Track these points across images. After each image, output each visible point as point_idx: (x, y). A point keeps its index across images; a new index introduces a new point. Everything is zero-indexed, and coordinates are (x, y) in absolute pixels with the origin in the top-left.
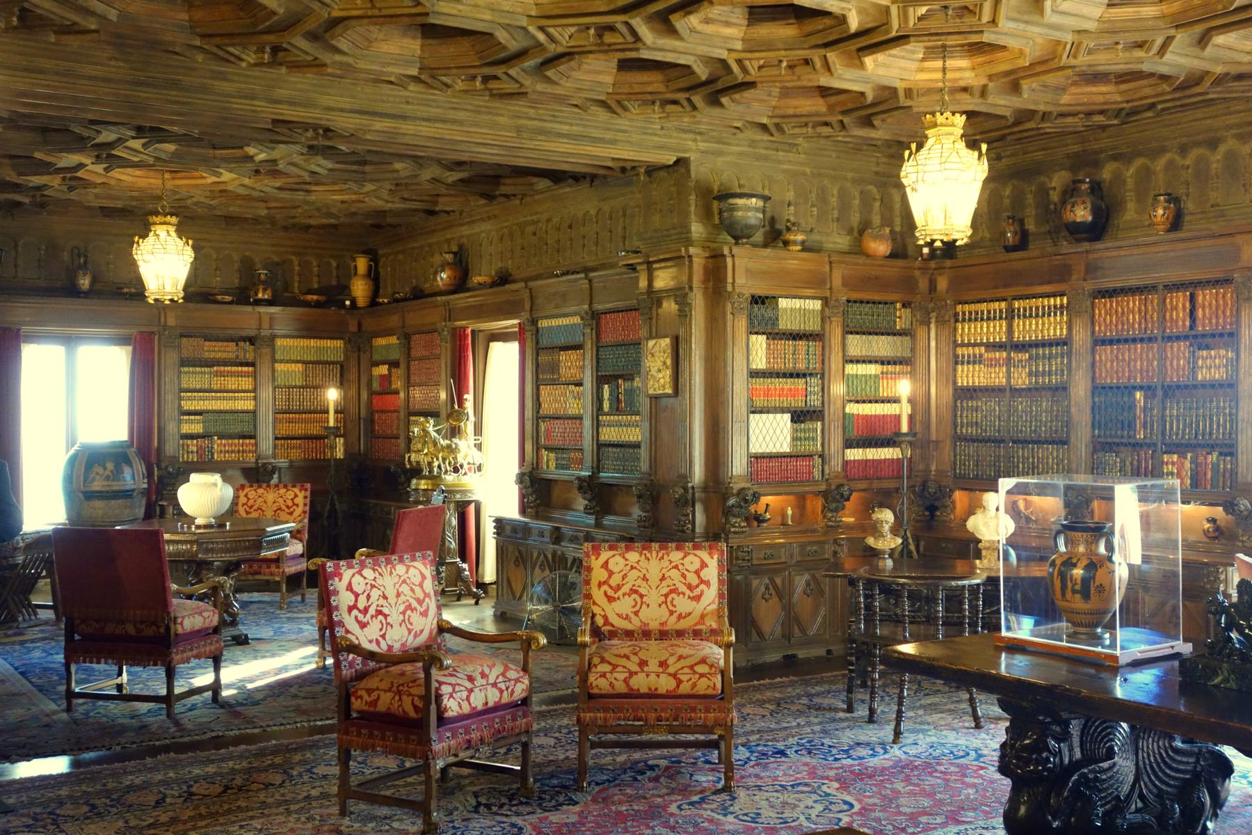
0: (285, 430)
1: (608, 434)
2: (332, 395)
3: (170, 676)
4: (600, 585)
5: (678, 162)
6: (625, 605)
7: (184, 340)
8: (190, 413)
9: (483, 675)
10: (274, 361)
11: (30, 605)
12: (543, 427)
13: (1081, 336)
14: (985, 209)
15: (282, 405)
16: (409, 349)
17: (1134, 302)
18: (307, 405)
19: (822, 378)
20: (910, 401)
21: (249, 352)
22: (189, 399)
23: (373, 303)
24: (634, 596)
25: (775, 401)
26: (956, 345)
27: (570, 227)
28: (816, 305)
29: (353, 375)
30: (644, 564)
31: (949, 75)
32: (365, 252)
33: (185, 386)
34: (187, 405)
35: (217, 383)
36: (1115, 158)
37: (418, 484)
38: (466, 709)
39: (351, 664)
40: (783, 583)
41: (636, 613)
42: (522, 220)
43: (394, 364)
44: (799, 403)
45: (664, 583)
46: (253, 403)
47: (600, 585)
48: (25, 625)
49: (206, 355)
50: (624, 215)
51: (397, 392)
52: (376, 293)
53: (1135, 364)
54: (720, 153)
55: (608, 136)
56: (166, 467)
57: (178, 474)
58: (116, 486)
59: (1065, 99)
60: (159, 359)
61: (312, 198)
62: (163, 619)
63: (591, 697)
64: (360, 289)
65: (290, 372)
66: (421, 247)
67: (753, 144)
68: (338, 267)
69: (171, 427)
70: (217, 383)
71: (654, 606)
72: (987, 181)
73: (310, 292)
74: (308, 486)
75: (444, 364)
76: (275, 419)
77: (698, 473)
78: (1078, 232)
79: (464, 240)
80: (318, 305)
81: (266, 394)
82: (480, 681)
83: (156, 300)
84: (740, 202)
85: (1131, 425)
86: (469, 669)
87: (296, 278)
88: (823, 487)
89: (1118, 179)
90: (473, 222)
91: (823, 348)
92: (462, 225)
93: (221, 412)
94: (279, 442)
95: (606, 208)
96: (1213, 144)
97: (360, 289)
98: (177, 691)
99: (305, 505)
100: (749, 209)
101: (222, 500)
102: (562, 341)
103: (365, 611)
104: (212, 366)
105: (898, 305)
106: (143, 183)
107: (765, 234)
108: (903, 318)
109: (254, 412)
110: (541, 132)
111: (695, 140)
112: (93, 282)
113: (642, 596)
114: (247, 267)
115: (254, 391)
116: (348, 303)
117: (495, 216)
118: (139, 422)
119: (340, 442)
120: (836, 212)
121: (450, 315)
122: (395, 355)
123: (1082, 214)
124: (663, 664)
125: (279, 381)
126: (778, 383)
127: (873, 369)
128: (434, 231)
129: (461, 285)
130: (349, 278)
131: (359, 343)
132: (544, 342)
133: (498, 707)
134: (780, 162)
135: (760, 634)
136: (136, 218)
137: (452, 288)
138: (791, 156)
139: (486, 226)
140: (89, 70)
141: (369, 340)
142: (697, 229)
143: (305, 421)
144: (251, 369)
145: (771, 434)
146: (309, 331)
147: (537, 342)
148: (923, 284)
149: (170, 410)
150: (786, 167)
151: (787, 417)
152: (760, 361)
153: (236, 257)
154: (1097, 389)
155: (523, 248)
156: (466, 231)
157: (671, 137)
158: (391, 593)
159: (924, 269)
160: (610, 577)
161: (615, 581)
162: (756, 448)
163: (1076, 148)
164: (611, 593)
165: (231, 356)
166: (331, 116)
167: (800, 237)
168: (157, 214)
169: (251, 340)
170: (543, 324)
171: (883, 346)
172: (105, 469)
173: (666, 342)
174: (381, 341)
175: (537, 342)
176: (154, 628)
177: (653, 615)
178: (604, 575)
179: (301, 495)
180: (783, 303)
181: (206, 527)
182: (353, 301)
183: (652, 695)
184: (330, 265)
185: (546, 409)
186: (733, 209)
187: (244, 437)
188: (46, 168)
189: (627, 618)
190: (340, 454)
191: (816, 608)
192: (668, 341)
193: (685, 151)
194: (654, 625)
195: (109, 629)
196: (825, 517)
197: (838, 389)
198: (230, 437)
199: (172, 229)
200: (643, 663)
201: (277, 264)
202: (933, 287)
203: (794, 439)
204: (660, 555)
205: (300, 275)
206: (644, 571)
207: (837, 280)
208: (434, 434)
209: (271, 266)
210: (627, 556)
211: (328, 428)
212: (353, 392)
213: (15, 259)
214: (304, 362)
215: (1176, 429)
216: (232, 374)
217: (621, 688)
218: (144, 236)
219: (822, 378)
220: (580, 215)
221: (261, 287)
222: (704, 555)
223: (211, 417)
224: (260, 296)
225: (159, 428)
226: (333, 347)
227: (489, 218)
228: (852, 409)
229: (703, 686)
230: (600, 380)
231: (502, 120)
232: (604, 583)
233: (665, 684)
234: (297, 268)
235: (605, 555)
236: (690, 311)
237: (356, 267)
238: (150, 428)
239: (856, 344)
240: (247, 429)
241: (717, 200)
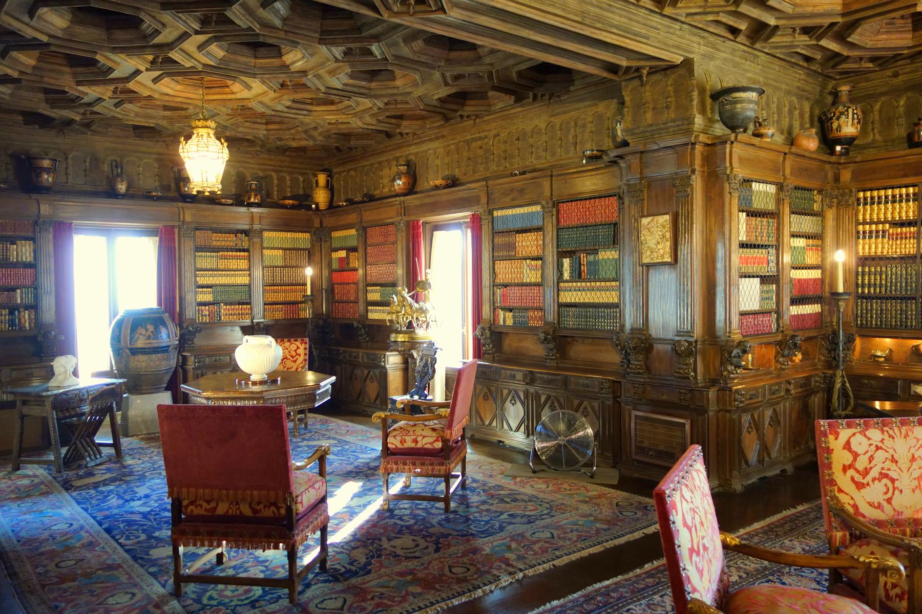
0: (272, 297)
1: (568, 297)
4: (845, 469)
6: (876, 492)
7: (198, 232)
8: (203, 287)
10: (263, 248)
11: (93, 442)
12: (499, 292)
16: (366, 238)
18: (286, 280)
19: (777, 250)
21: (244, 242)
22: (202, 276)
23: (331, 206)
24: (885, 481)
27: (518, 139)
30: (888, 442)
32: (323, 170)
33: (198, 266)
34: (201, 281)
35: (222, 264)
37: (396, 337)
40: (759, 417)
41: (889, 501)
42: (469, 137)
45: (915, 465)
46: (248, 278)
47: (845, 469)
48: (93, 464)
49: (214, 243)
50: (576, 125)
51: (356, 270)
56: (187, 327)
57: (196, 332)
58: (155, 343)
60: (179, 247)
62: (285, 499)
64: (321, 197)
65: (274, 256)
66: (372, 165)
68: (304, 182)
69: (189, 297)
70: (222, 264)
71: (907, 491)
73: (285, 198)
74: (307, 340)
76: (264, 290)
79: (412, 157)
81: (258, 273)
83: (198, 192)
87: (275, 189)
88: (779, 338)
90: (424, 142)
91: (779, 224)
92: (410, 145)
93: (221, 285)
94: (267, 307)
95: (557, 121)
97: (321, 197)
99: (305, 354)
101: (275, 358)
102: (519, 226)
104: (218, 252)
105: (815, 192)
111: (699, 44)
112: (128, 188)
113: (893, 481)
115: (249, 269)
116: (314, 206)
117: (443, 136)
118: (165, 294)
120: (776, 116)
121: (406, 210)
122: (353, 243)
128: (384, 152)
130: (312, 189)
131: (321, 235)
132: (499, 227)
134: (746, 70)
135: (747, 462)
137: (405, 191)
143: (285, 291)
144: (246, 254)
146: (286, 226)
147: (493, 228)
150: (750, 75)
151: (757, 280)
155: (469, 159)
156: (413, 149)
157: (683, 38)
160: (855, 460)
161: (862, 463)
164: (858, 478)
165: (232, 244)
169: (246, 233)
172: (147, 330)
175: (493, 228)
176: (273, 508)
178: (847, 458)
179: (302, 347)
180: (755, 186)
181: (262, 383)
182: (317, 205)
184: (298, 179)
187: (243, 304)
188: (102, 75)
189: (879, 506)
191: (775, 435)
192: (667, 217)
193: (691, 52)
196: (777, 361)
197: (787, 259)
198: (231, 304)
199: (212, 132)
201: (262, 178)
202: (837, 179)
203: (762, 299)
204: (904, 432)
205: (278, 186)
206: (891, 452)
208: (410, 300)
210: (868, 433)
213: (66, 168)
214: (284, 249)
216: (233, 258)
218: (188, 137)
219: (777, 250)
220: (529, 129)
221: (253, 194)
223: (219, 289)
224: (252, 200)
225: (181, 298)
227: (437, 138)
230: (562, 255)
232: (851, 466)
234: (276, 182)
235: (845, 434)
236: (692, 191)
237: (317, 181)
238: (174, 298)
240: (244, 298)
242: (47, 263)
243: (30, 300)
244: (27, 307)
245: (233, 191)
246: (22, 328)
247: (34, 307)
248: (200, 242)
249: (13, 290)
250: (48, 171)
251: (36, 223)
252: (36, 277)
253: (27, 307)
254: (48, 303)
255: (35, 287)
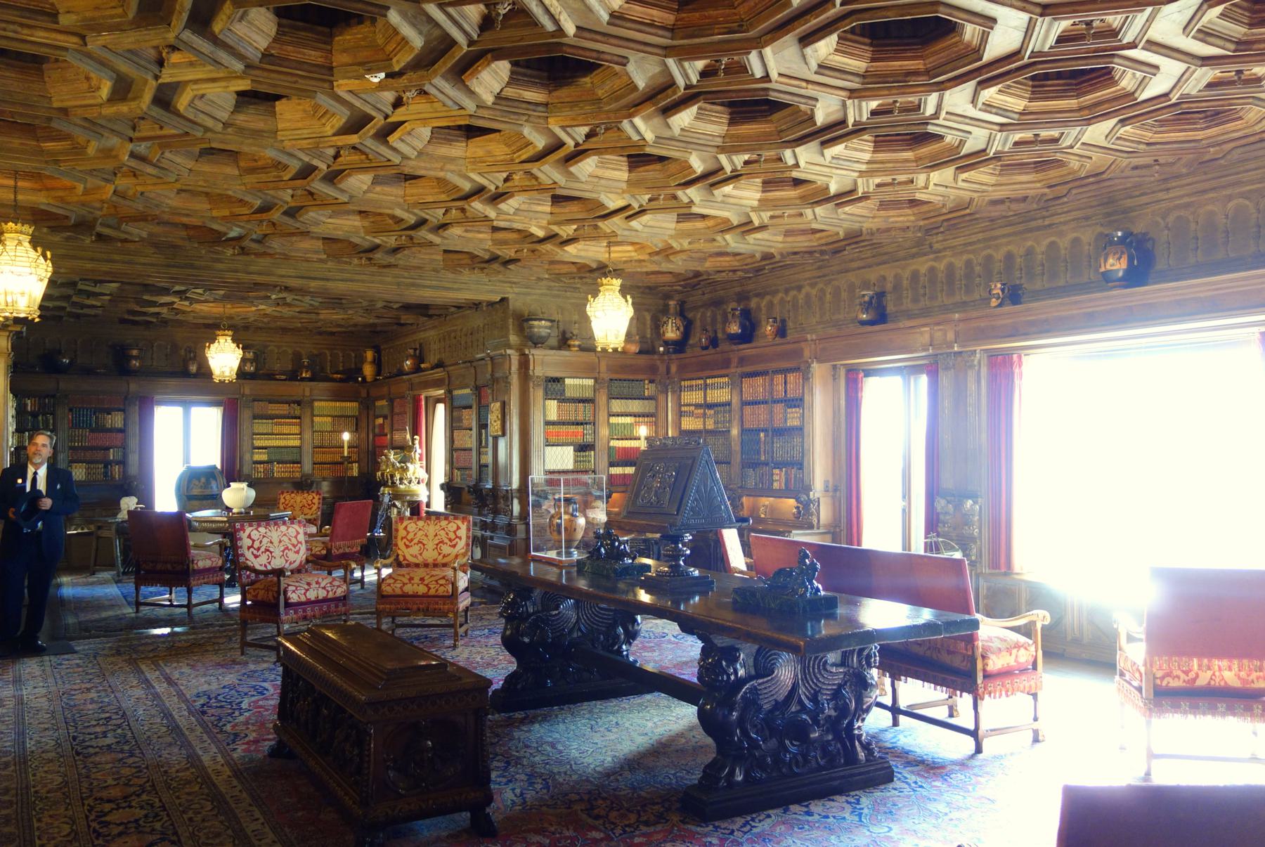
0: (319, 458)
2: (346, 436)
3: (190, 592)
5: (503, 300)
9: (317, 583)
13: (735, 401)
14: (634, 331)
15: (317, 443)
17: (760, 380)
20: (646, 438)
21: (297, 410)
25: (563, 439)
26: (681, 406)
28: (591, 382)
29: (364, 424)
31: (612, 255)
34: (257, 443)
35: (277, 429)
36: (757, 295)
38: (303, 599)
39: (248, 577)
43: (385, 417)
44: (579, 439)
52: (378, 373)
53: (756, 417)
54: (529, 294)
55: (456, 286)
58: (208, 492)
59: (707, 264)
61: (322, 317)
63: (383, 596)
64: (368, 370)
65: (323, 422)
67: (549, 288)
69: (247, 457)
70: (277, 429)
72: (632, 319)
73: (337, 373)
75: (408, 418)
77: (515, 484)
78: (733, 338)
80: (341, 380)
82: (314, 585)
84: (536, 323)
85: (759, 453)
86: (309, 580)
89: (759, 308)
96: (799, 288)
97: (368, 370)
98: (194, 602)
100: (540, 327)
101: (247, 498)
103: (258, 549)
106: (215, 310)
107: (559, 341)
108: (649, 389)
109: (300, 447)
110: (413, 285)
114: (297, 357)
119: (355, 466)
122: (386, 411)
123: (734, 328)
124: (422, 579)
125: (316, 428)
126: (564, 428)
127: (629, 420)
129: (417, 369)
131: (367, 405)
132: (456, 404)
133: (325, 600)
136: (210, 330)
138: (576, 295)
139: (432, 333)
140: (142, 260)
141: (374, 402)
142: (513, 339)
145: (562, 458)
146: (337, 397)
148: (662, 369)
149: (246, 446)
151: (572, 448)
152: (553, 415)
153: (290, 351)
154: (744, 431)
156: (422, 335)
158: (276, 541)
159: (663, 361)
161: (409, 537)
162: (550, 467)
163: (738, 289)
166: (284, 280)
167: (577, 343)
168: (220, 329)
170: (456, 393)
171: (635, 406)
173: (498, 404)
174: (379, 403)
177: (430, 555)
183: (415, 596)
185: (457, 444)
186: (531, 327)
190: (355, 473)
194: (430, 561)
195: (159, 567)
197: (604, 432)
199: (229, 339)
200: (411, 579)
207: (603, 368)
209: (312, 357)
211: (343, 457)
212: (364, 435)
215: (779, 455)
216: (287, 424)
217: (398, 592)
222: (459, 522)
226: (352, 407)
228: (614, 443)
229: (441, 591)
231: (389, 279)
233: (422, 589)
238: (234, 457)
239: (617, 405)
240: (295, 457)
241: (523, 321)
242: (134, 429)
243: (119, 457)
244: (118, 463)
245: (290, 367)
246: (113, 478)
247: (123, 463)
248: (257, 411)
249: (108, 449)
250: (136, 358)
251: (126, 398)
252: (125, 440)
253: (118, 463)
254: (133, 459)
255: (124, 447)
